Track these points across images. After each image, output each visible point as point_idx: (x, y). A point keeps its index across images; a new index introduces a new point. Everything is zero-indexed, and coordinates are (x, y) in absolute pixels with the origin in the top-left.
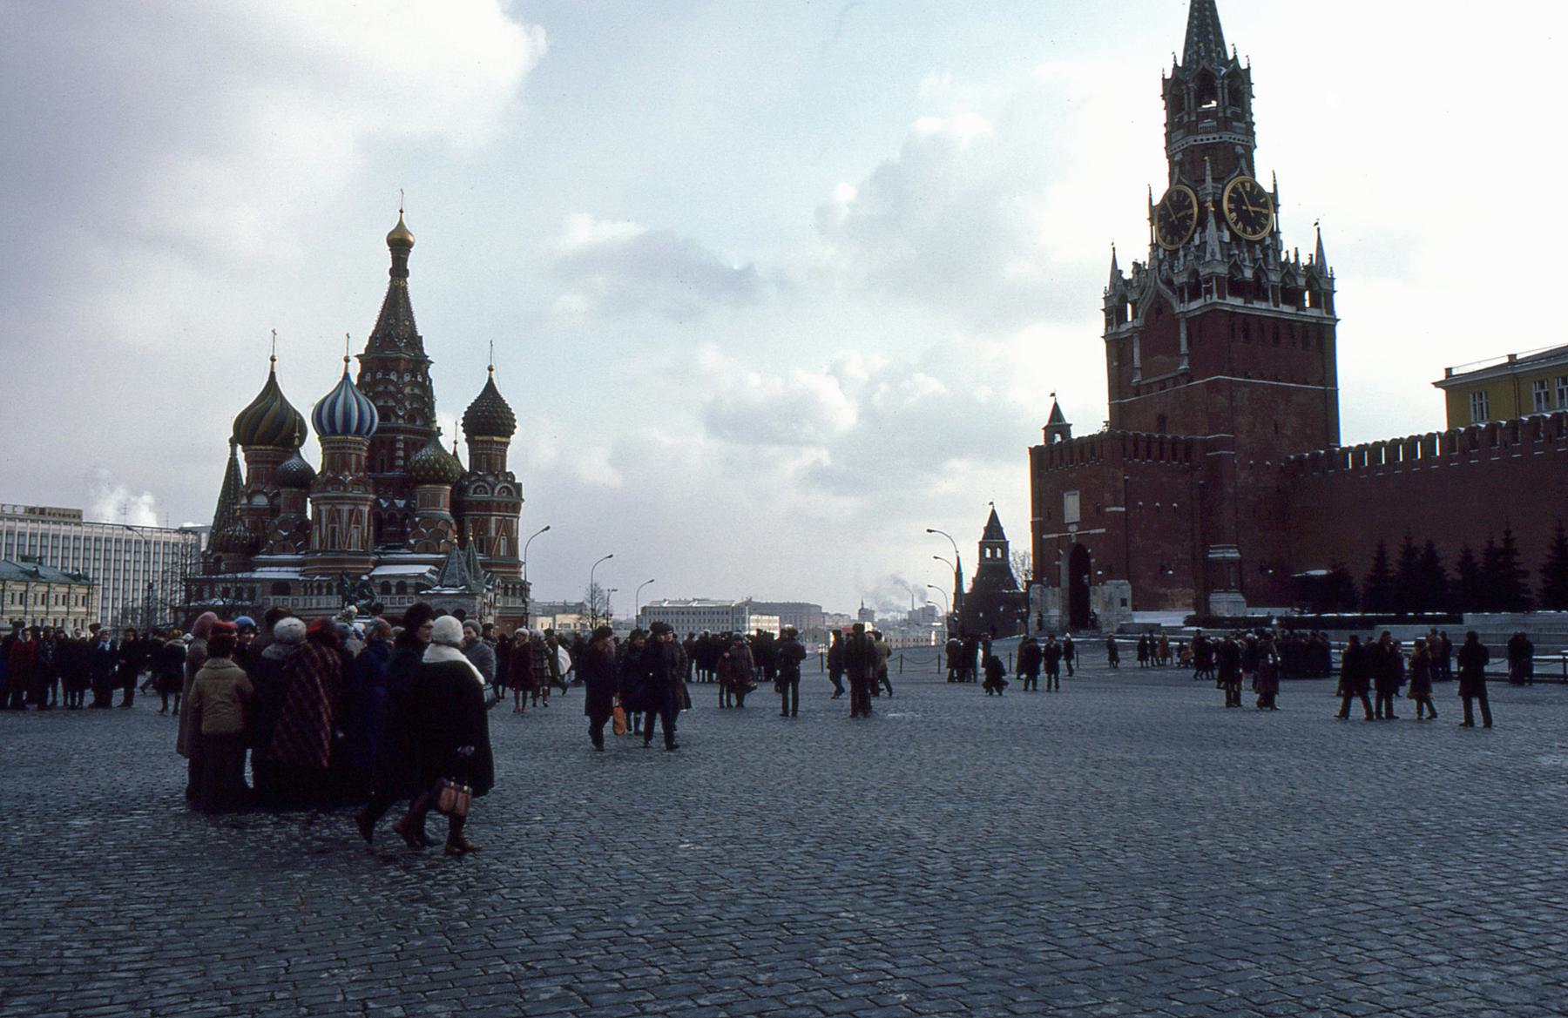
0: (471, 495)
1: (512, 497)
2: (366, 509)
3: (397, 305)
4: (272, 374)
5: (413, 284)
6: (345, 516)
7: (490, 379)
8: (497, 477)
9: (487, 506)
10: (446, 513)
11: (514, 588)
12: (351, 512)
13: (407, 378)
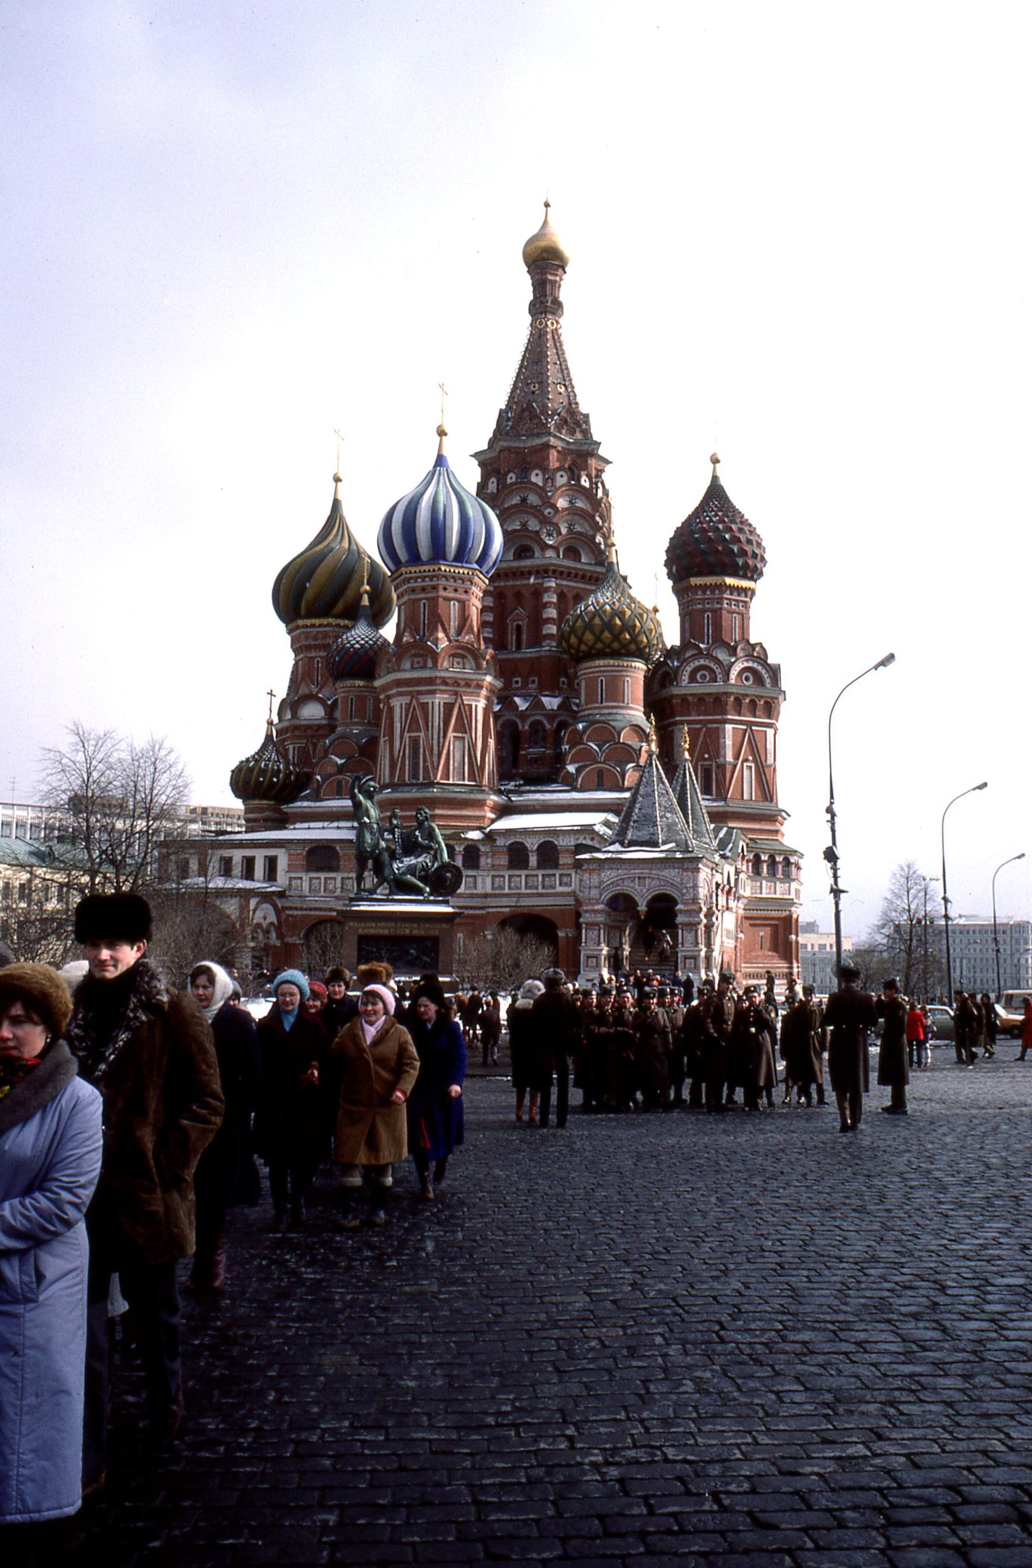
0: (684, 686)
1: (764, 690)
2: (480, 704)
3: (540, 359)
4: (336, 505)
5: (572, 328)
6: (437, 718)
7: (715, 478)
8: (733, 651)
9: (716, 704)
10: (637, 713)
11: (773, 863)
12: (448, 708)
13: (561, 479)
